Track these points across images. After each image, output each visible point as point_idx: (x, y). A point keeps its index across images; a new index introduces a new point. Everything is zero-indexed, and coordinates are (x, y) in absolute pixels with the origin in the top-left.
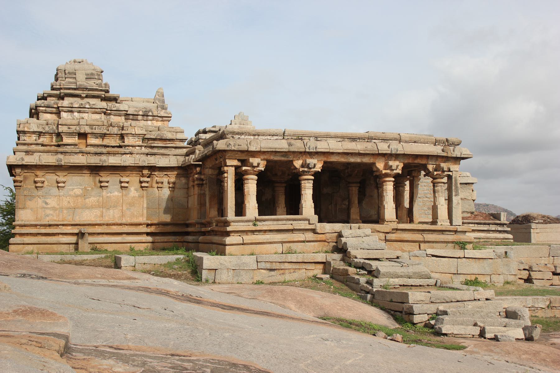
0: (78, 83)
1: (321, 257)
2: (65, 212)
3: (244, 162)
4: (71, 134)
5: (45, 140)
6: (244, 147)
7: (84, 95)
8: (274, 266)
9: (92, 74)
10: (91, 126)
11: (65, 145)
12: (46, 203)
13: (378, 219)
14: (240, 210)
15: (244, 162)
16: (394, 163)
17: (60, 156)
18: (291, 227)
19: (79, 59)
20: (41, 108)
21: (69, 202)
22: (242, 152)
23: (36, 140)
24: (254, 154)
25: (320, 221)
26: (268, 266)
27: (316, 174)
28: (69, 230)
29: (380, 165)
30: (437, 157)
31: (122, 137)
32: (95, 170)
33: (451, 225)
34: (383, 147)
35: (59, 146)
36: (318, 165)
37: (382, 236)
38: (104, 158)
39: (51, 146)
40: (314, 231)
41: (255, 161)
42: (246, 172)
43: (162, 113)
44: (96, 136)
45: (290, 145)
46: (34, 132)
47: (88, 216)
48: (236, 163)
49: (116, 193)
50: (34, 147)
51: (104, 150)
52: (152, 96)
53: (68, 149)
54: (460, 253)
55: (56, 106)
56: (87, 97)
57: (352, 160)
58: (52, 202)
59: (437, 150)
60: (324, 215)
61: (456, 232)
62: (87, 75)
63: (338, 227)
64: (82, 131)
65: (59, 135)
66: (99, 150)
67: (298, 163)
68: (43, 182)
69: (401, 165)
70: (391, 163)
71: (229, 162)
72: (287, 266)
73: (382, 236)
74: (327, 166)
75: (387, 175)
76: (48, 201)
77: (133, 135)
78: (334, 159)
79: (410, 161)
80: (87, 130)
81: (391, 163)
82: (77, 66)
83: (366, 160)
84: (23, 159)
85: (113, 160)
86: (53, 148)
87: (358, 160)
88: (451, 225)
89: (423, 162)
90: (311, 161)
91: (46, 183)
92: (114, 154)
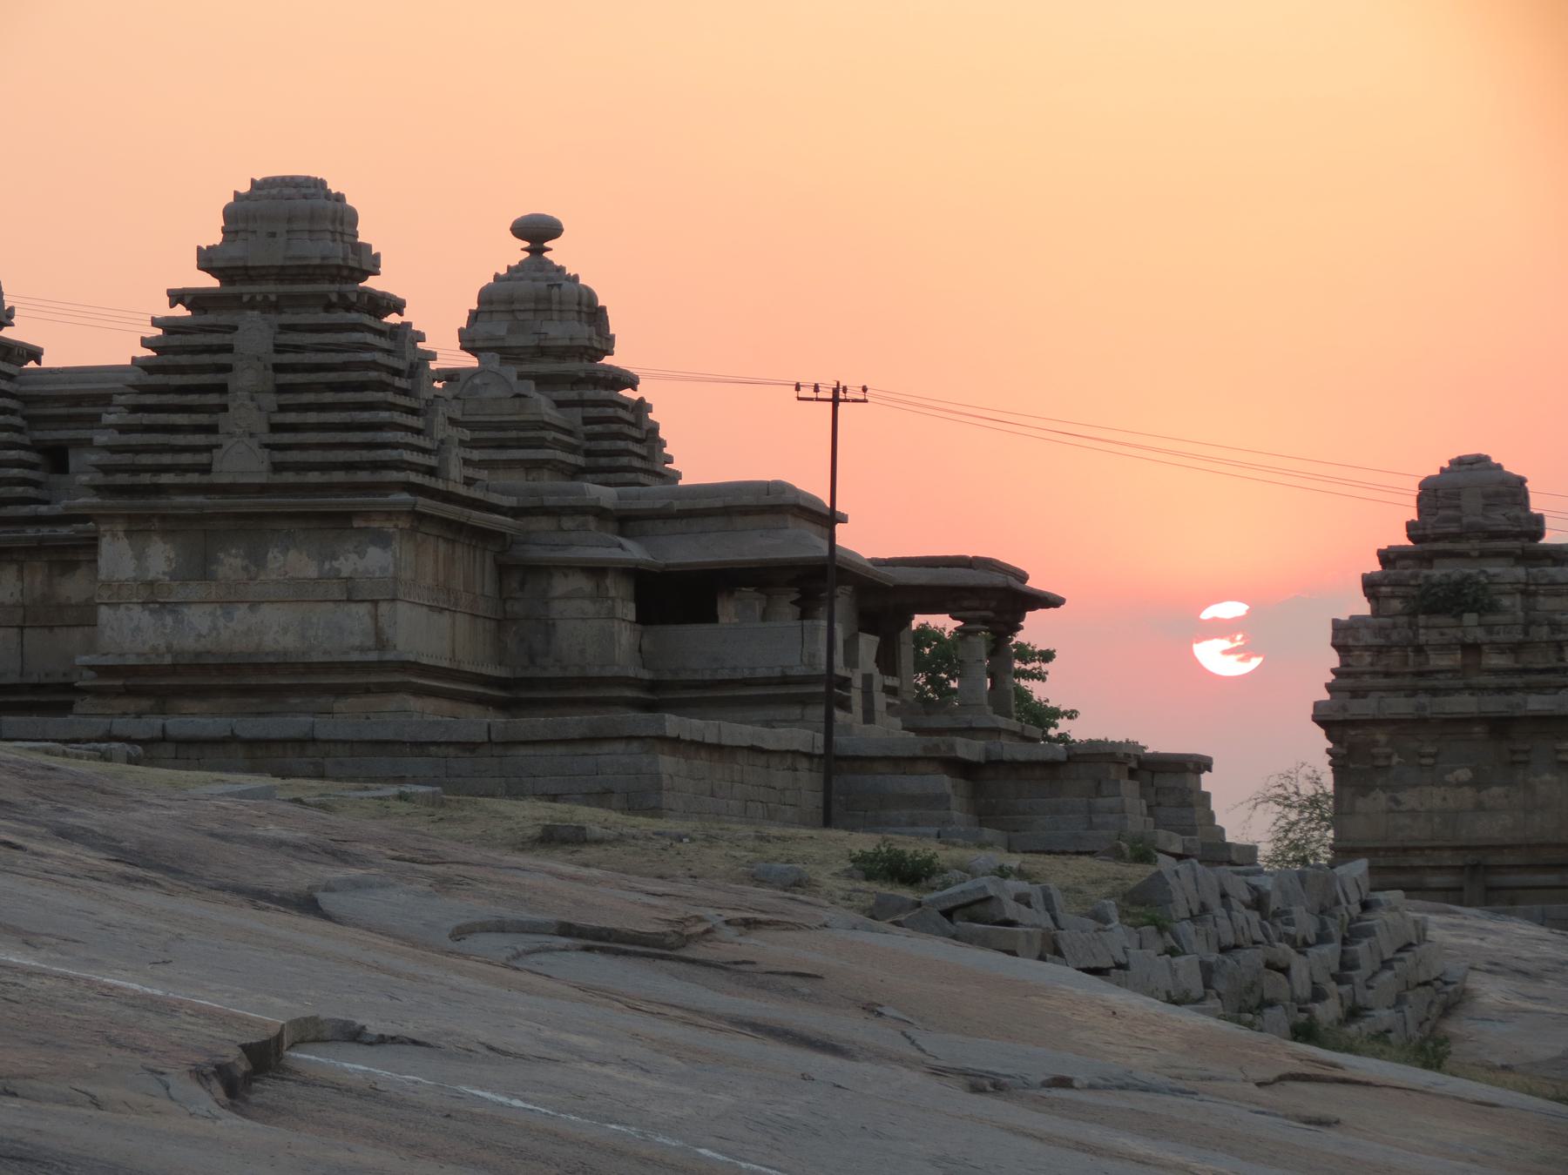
0: (1465, 520)
2: (1437, 820)
7: (1476, 553)
9: (1498, 495)
11: (1432, 672)
12: (1397, 802)
17: (1424, 699)
20: (1383, 589)
21: (1444, 799)
23: (1372, 664)
28: (1447, 859)
32: (1500, 726)
35: (1420, 674)
38: (1516, 698)
39: (1404, 674)
44: (1500, 649)
46: (1367, 648)
47: (1487, 829)
49: (1548, 777)
50: (1368, 681)
51: (1518, 681)
53: (1441, 682)
55: (1412, 582)
56: (1483, 555)
58: (1409, 799)
62: (1486, 496)
64: (1469, 639)
65: (1419, 649)
66: (1507, 681)
68: (1389, 757)
76: (1402, 796)
84: (1344, 708)
85: (1537, 704)
86: (1407, 681)
91: (1395, 759)
92: (1540, 689)
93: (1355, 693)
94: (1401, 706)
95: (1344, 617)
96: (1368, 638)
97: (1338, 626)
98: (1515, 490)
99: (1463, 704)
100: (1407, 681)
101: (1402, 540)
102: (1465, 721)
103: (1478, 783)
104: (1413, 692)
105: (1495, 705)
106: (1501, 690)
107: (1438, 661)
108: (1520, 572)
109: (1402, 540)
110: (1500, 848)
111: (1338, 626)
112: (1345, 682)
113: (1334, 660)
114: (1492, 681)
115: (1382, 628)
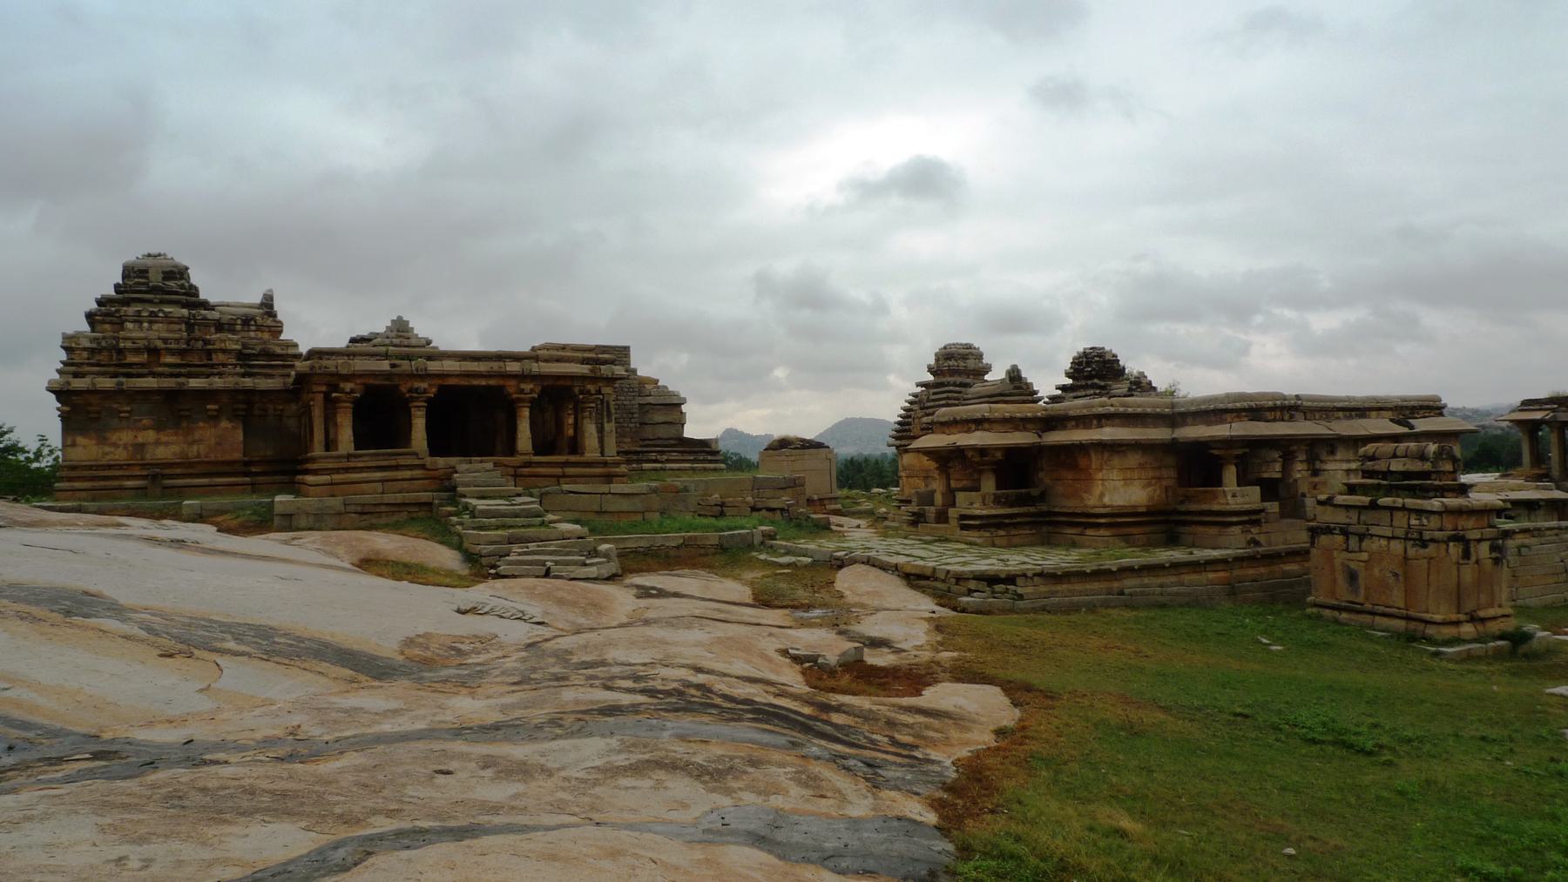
1: (425, 496)
3: (336, 388)
4: (137, 351)
5: (103, 358)
6: (333, 369)
8: (367, 509)
9: (171, 272)
10: (165, 340)
13: (511, 450)
14: (330, 444)
15: (336, 388)
16: (527, 387)
18: (393, 463)
19: (154, 251)
22: (332, 375)
24: (348, 378)
25: (432, 454)
26: (359, 509)
27: (429, 400)
29: (511, 386)
30: (583, 378)
31: (209, 353)
32: (171, 396)
33: (602, 454)
34: (513, 367)
36: (429, 388)
37: (511, 471)
40: (423, 467)
41: (348, 386)
42: (337, 400)
43: (269, 322)
44: (172, 352)
45: (393, 366)
46: (85, 349)
48: (324, 389)
52: (257, 300)
54: (604, 488)
56: (162, 302)
57: (475, 382)
59: (584, 369)
60: (436, 448)
61: (605, 464)
63: (453, 460)
65: (120, 351)
67: (404, 389)
69: (538, 389)
70: (523, 386)
71: (315, 388)
72: (383, 508)
73: (511, 471)
74: (441, 388)
75: (520, 400)
77: (224, 351)
78: (452, 381)
79: (551, 383)
80: (159, 344)
81: (523, 386)
82: (150, 262)
83: (492, 382)
84: (68, 383)
85: (194, 383)
86: (112, 369)
87: (484, 383)
88: (602, 454)
89: (568, 383)
90: (424, 385)
93: (76, 375)
94: (107, 383)
95: (70, 331)
96: (87, 344)
97: (66, 337)
98: (179, 273)
99: (150, 383)
100: (112, 369)
101: (111, 292)
102: (146, 394)
103: (159, 428)
104: (115, 375)
105: (169, 383)
106: (172, 375)
107: (132, 359)
108: (185, 312)
109: (111, 292)
110: (171, 465)
111: (66, 337)
112: (71, 367)
113: (63, 356)
114: (167, 370)
115: (96, 339)
